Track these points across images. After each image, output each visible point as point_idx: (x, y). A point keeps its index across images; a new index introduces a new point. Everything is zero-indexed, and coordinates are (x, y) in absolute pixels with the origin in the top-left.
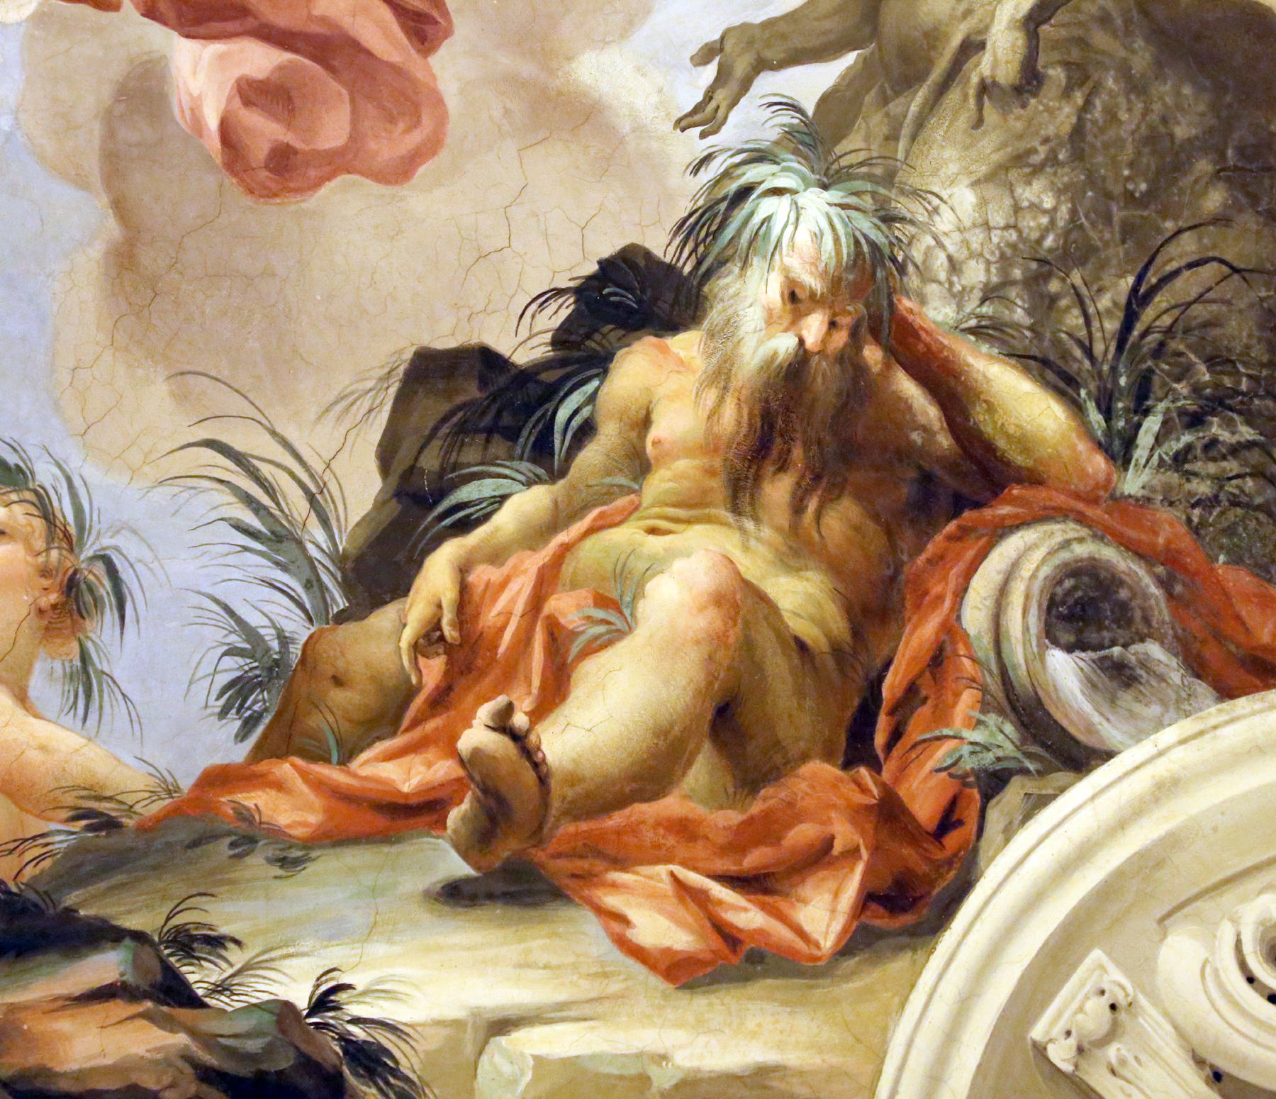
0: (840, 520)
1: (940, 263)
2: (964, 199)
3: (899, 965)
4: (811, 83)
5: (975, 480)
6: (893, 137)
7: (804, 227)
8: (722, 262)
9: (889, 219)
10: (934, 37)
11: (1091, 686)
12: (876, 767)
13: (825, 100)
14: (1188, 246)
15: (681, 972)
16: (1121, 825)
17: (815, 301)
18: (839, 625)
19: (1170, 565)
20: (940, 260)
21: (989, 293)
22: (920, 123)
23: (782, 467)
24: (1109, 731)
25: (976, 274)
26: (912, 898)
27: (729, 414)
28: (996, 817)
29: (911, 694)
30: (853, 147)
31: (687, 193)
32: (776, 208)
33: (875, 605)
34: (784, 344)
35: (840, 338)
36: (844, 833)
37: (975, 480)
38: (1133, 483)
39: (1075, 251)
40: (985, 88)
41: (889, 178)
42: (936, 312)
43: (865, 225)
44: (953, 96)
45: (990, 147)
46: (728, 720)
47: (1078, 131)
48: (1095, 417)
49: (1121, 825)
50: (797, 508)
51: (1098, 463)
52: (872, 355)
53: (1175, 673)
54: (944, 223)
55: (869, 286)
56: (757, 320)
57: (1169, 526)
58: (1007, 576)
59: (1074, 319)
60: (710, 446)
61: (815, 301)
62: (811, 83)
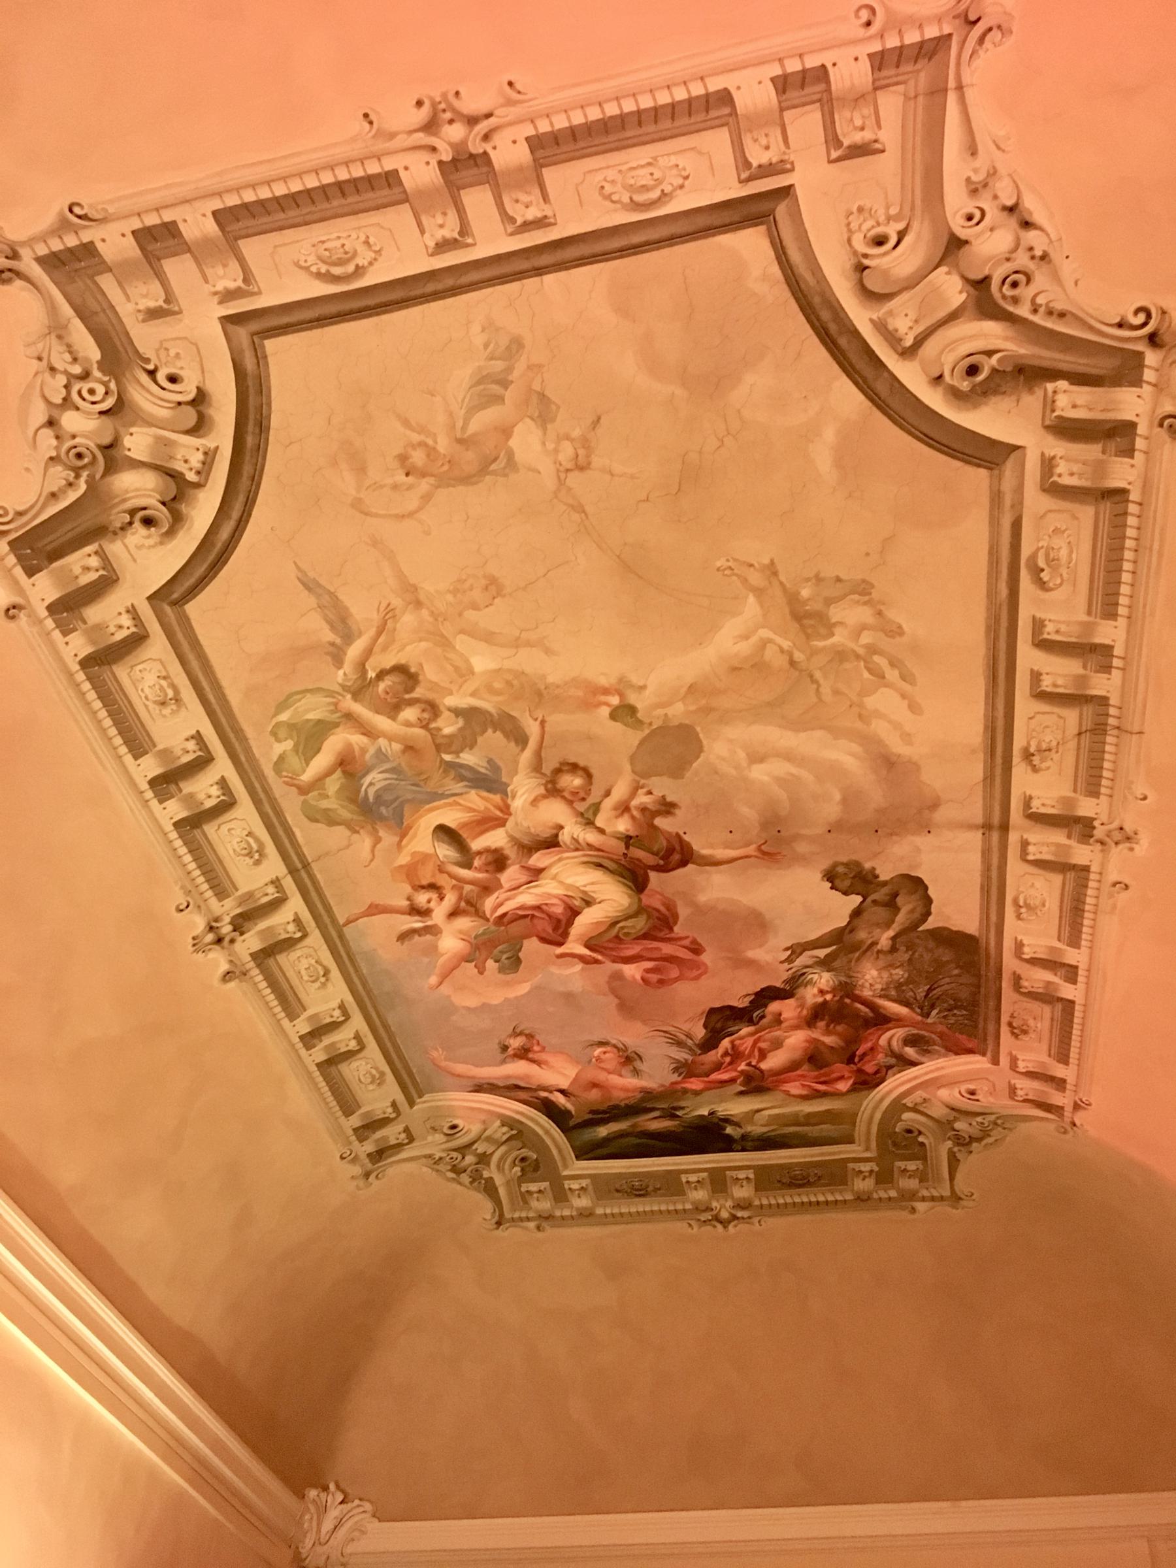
0: (840, 1028)
1: (867, 985)
2: (874, 973)
3: (866, 1092)
4: (822, 953)
5: (882, 1020)
6: (850, 961)
7: (825, 979)
8: (798, 987)
9: (851, 977)
10: (862, 942)
11: (917, 1052)
12: (854, 1063)
13: (827, 956)
14: (947, 980)
15: (804, 1098)
16: (926, 1073)
17: (828, 992)
18: (842, 1044)
19: (941, 1035)
20: (867, 985)
21: (882, 990)
22: (858, 959)
23: (822, 1020)
24: (923, 1059)
25: (879, 986)
26: (867, 1082)
27: (805, 1012)
28: (890, 1072)
29: (864, 1054)
30: (837, 964)
31: (786, 976)
32: (816, 977)
33: (852, 1042)
34: (820, 1000)
35: (837, 998)
36: (847, 1074)
37: (882, 1020)
38: (929, 1021)
39: (908, 981)
40: (879, 952)
41: (850, 969)
42: (867, 993)
43: (843, 979)
44: (869, 953)
45: (881, 963)
46: (814, 1058)
47: (910, 960)
48: (918, 1011)
49: (926, 1073)
50: (828, 1026)
51: (919, 1018)
52: (847, 1001)
53: (943, 1051)
54: (867, 977)
55: (846, 990)
56: (810, 995)
57: (940, 1028)
58: (893, 1037)
59: (911, 994)
60: (799, 1017)
61: (828, 992)
62: (822, 953)
